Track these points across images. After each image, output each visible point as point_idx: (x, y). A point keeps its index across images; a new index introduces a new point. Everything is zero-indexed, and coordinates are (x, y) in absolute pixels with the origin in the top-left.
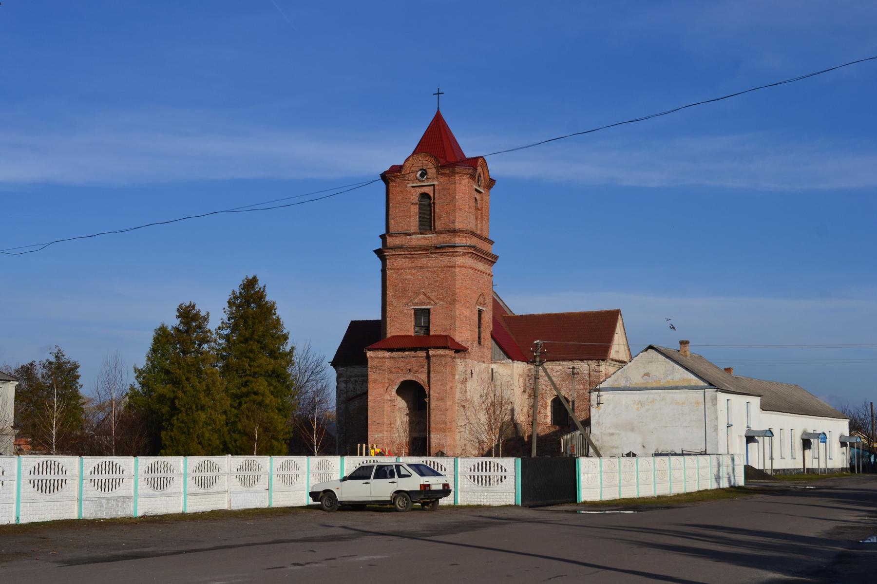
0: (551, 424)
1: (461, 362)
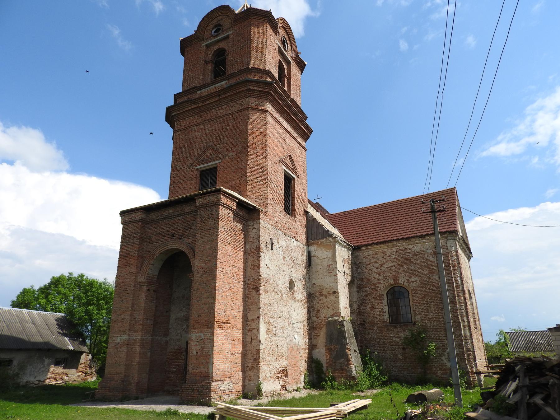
0: (390, 323)
1: (253, 225)
